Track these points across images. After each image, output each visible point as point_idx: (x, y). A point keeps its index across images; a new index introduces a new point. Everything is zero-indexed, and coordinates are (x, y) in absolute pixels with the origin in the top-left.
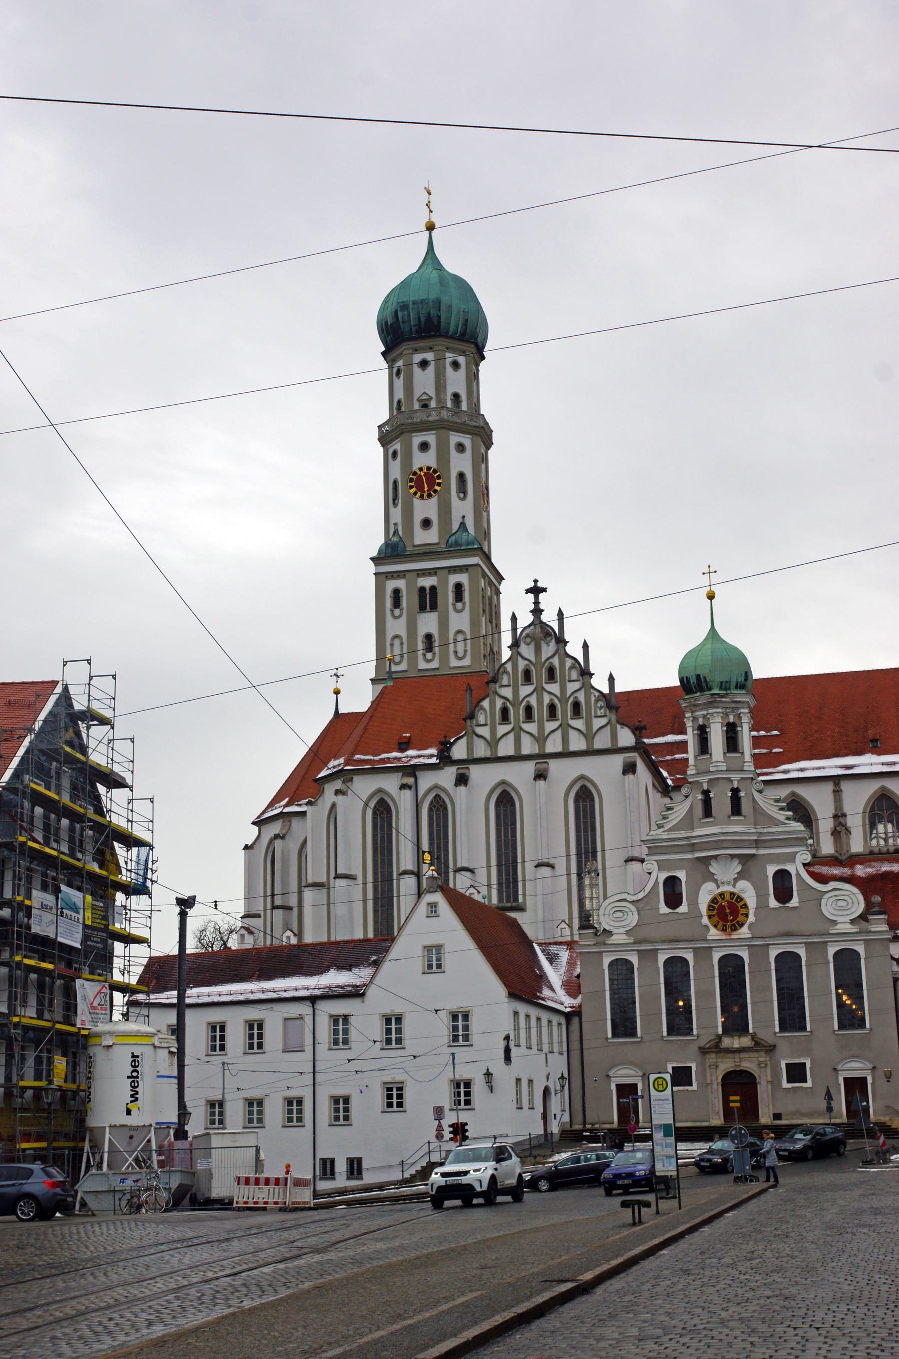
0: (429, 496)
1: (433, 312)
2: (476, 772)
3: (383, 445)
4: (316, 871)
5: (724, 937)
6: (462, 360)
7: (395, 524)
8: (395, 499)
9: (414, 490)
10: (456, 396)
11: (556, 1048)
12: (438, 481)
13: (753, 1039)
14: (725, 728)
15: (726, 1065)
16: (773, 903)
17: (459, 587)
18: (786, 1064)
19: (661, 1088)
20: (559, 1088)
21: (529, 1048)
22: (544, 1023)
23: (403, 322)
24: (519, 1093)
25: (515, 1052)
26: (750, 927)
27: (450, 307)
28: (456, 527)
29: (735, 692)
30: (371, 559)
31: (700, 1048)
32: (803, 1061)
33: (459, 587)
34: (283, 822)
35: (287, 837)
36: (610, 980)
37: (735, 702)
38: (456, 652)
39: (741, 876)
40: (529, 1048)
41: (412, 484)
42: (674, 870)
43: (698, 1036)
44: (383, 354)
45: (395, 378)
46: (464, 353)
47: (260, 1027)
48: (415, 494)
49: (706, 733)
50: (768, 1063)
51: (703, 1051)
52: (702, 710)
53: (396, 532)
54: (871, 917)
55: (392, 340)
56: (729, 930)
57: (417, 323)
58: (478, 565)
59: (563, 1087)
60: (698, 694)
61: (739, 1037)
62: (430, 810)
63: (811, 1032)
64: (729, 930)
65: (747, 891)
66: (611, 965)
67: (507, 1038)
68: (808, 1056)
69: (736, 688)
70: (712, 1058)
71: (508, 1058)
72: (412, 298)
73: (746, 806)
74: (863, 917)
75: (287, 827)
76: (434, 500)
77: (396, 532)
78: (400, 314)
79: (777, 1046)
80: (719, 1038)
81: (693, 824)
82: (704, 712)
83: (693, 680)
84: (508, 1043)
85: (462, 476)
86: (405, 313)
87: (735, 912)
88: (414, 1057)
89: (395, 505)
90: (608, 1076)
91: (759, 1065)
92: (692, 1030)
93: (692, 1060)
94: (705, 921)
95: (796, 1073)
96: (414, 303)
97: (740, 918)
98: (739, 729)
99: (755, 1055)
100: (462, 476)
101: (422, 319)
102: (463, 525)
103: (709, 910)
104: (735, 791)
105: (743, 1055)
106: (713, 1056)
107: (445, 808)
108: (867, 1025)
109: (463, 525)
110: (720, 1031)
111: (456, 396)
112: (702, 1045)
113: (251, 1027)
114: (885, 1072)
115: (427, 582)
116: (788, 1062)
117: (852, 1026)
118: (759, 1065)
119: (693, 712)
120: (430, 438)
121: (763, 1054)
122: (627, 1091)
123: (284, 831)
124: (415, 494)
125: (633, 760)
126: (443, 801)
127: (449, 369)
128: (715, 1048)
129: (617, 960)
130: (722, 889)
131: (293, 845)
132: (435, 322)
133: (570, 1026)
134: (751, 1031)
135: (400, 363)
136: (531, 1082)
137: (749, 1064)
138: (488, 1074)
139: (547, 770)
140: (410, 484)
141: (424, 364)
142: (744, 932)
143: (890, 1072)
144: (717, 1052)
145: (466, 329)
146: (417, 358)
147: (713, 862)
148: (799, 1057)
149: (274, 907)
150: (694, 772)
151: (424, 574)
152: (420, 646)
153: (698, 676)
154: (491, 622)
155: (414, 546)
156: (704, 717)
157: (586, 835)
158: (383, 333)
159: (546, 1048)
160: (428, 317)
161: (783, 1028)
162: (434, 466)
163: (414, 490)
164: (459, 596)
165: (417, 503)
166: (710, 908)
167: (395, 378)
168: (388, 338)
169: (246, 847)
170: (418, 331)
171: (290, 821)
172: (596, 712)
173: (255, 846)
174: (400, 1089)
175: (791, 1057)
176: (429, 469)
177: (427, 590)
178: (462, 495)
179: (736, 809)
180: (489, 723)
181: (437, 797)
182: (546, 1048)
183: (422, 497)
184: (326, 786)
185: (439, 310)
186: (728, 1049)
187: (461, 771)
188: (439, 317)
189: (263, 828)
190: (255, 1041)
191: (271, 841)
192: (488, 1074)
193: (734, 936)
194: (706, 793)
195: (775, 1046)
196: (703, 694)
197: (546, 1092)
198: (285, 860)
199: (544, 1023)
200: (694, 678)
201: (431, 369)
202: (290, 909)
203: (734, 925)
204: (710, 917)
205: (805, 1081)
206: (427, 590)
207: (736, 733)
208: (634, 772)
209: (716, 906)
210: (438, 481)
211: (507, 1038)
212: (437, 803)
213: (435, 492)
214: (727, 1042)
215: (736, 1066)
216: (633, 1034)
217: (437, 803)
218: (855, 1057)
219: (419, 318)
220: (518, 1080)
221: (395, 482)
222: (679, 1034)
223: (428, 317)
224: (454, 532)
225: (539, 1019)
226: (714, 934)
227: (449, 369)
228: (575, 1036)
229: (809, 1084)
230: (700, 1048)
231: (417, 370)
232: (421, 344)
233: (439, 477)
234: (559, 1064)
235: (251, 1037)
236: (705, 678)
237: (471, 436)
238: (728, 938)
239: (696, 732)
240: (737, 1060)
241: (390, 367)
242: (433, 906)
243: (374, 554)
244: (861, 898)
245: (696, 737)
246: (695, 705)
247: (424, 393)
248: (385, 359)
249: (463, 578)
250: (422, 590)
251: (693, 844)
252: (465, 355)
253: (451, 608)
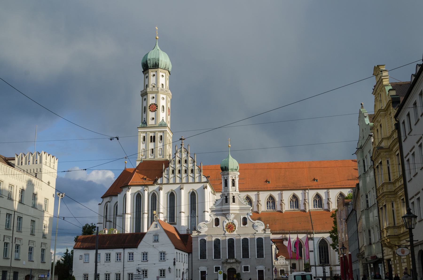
1: (157, 62)
2: (164, 187)
3: (142, 97)
4: (120, 212)
5: (229, 234)
6: (164, 75)
7: (144, 118)
8: (144, 112)
11: (186, 262)
13: (235, 260)
14: (232, 180)
15: (228, 267)
16: (242, 225)
18: (244, 267)
19: (220, 273)
20: (186, 272)
21: (180, 262)
22: (183, 255)
23: (149, 64)
24: (177, 273)
25: (176, 263)
26: (236, 232)
27: (162, 61)
28: (161, 120)
29: (234, 171)
31: (222, 262)
32: (248, 266)
33: (161, 136)
34: (110, 198)
35: (111, 202)
36: (200, 244)
37: (235, 174)
38: (159, 154)
39: (235, 218)
40: (180, 262)
42: (218, 216)
43: (222, 259)
44: (143, 72)
45: (146, 79)
47: (110, 255)
49: (227, 181)
50: (239, 266)
51: (223, 263)
52: (226, 175)
53: (145, 120)
54: (266, 230)
55: (145, 68)
56: (231, 232)
57: (153, 64)
58: (167, 131)
59: (187, 271)
60: (225, 171)
61: (232, 259)
62: (152, 197)
63: (250, 258)
64: (231, 232)
65: (236, 222)
66: (200, 240)
67: (174, 259)
68: (249, 264)
69: (235, 170)
70: (225, 265)
71: (174, 264)
72: (151, 58)
73: (236, 200)
74: (264, 230)
75: (111, 199)
77: (145, 120)
78: (148, 62)
79: (242, 262)
80: (227, 259)
81: (222, 205)
82: (227, 176)
83: (224, 168)
84: (175, 260)
86: (150, 61)
87: (233, 228)
88: (155, 264)
89: (145, 113)
90: (198, 269)
91: (237, 267)
92: (220, 257)
93: (220, 265)
94: (225, 230)
95: (246, 269)
96: (152, 59)
97: (234, 229)
98: (235, 181)
99: (236, 264)
100: (163, 106)
101: (154, 63)
102: (163, 119)
103: (226, 227)
104: (234, 197)
105: (233, 264)
106: (226, 264)
107: (156, 197)
108: (264, 257)
109: (163, 119)
110: (227, 258)
111: (163, 85)
112: (223, 261)
113: (107, 255)
114: (268, 269)
115: (152, 135)
116: (244, 266)
117: (260, 257)
118: (237, 267)
119: (224, 176)
120: (154, 95)
121: (238, 264)
122: (203, 273)
123: (110, 200)
125: (206, 185)
126: (155, 194)
127: (161, 77)
128: (226, 262)
129: (202, 239)
130: (229, 222)
131: (112, 204)
132: (157, 64)
133: (189, 256)
134: (235, 258)
135: (147, 75)
136: (180, 270)
137: (234, 266)
138: (169, 268)
139: (183, 187)
142: (235, 233)
143: (269, 269)
144: (226, 263)
145: (166, 67)
147: (227, 214)
148: (247, 265)
149: (106, 221)
150: (224, 191)
151: (152, 132)
152: (150, 152)
153: (225, 167)
154: (169, 146)
156: (227, 177)
157: (193, 205)
158: (143, 66)
159: (183, 262)
160: (156, 63)
161: (243, 258)
164: (161, 139)
165: (150, 112)
166: (226, 226)
167: (146, 79)
168: (145, 68)
169: (99, 204)
170: (153, 67)
171: (112, 197)
172: (196, 172)
173: (102, 204)
174: (146, 271)
175: (245, 265)
176: (154, 104)
177: (153, 137)
178: (163, 111)
179: (234, 201)
180: (168, 174)
181: (154, 193)
182: (183, 262)
183: (152, 111)
184: (123, 189)
185: (159, 61)
186: (229, 262)
187: (160, 187)
188: (159, 63)
189: (104, 199)
190: (108, 259)
191: (106, 203)
192: (169, 268)
193: (232, 233)
194: (226, 197)
195: (241, 262)
196: (227, 171)
197: (183, 273)
198: (110, 208)
199: (183, 255)
200: (224, 167)
202: (111, 222)
203: (232, 231)
204: (226, 229)
205: (248, 271)
206: (153, 137)
207: (234, 182)
208: (207, 189)
209: (228, 226)
211: (174, 259)
212: (154, 195)
214: (229, 261)
215: (231, 267)
216: (206, 258)
217: (154, 195)
218: (261, 265)
219: (153, 63)
220: (177, 270)
222: (217, 258)
223: (156, 63)
225: (182, 254)
226: (227, 233)
228: (190, 259)
229: (249, 272)
230: (222, 262)
234: (186, 266)
235: (107, 257)
236: (227, 167)
237: (166, 96)
238: (230, 234)
239: (224, 181)
240: (232, 265)
241: (145, 75)
242: (156, 225)
244: (264, 225)
245: (224, 182)
246: (224, 174)
248: (143, 73)
251: (222, 210)
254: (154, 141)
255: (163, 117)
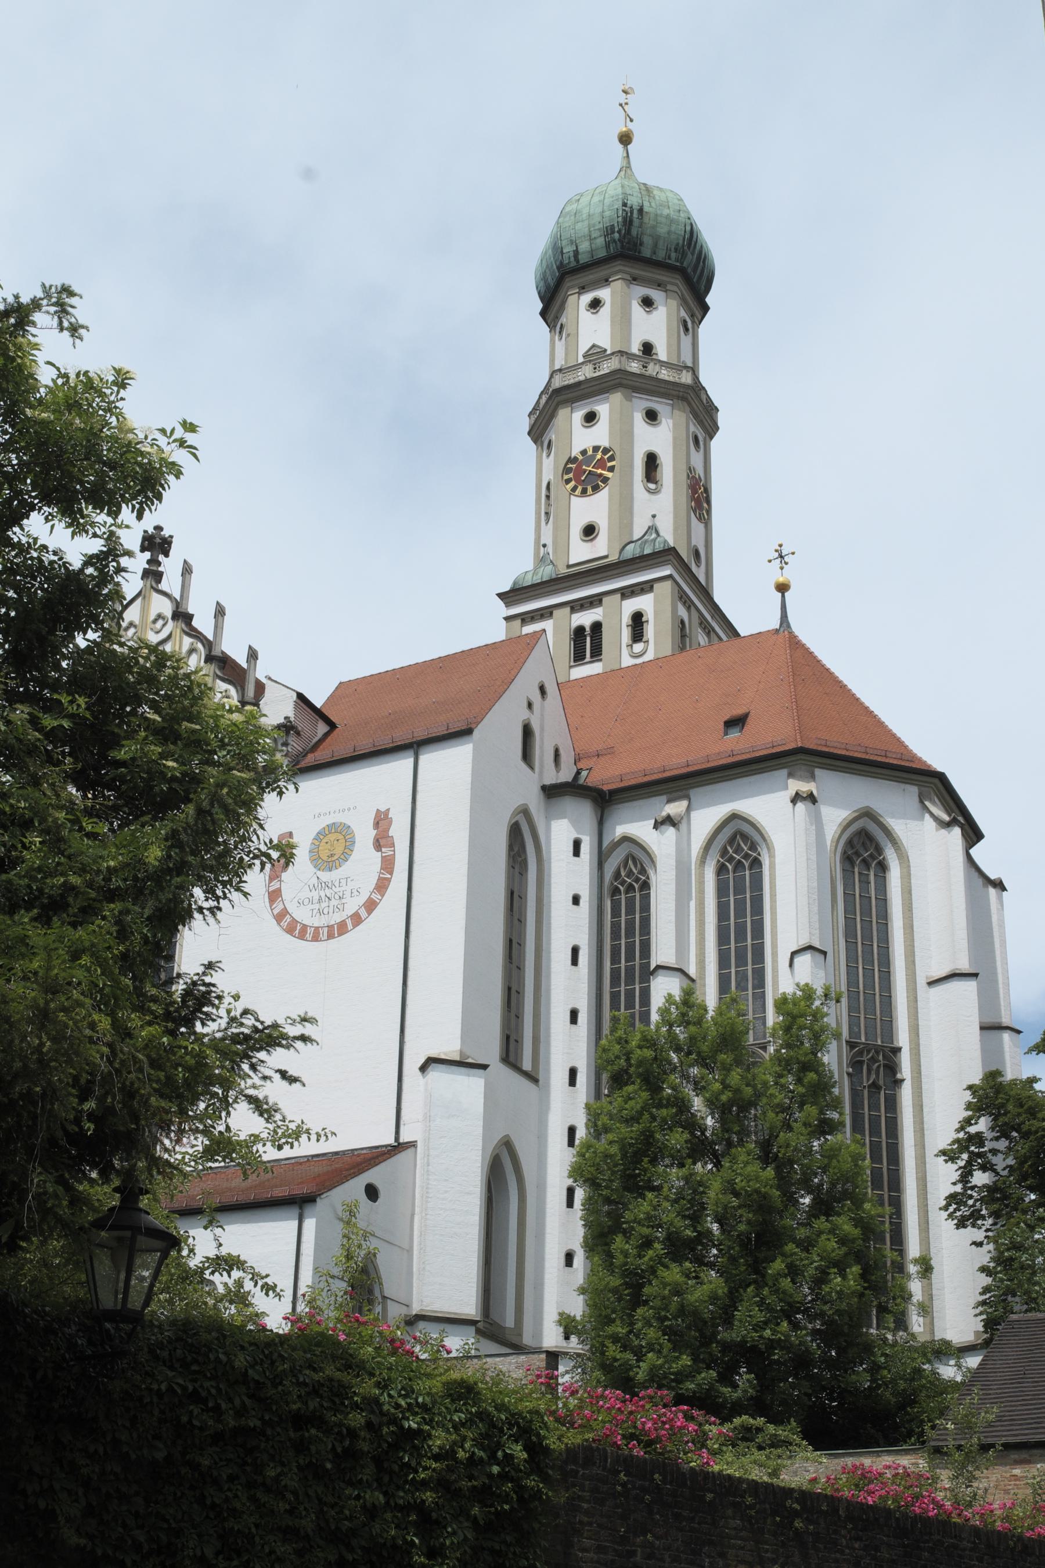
0: (596, 489)
3: (535, 442)
9: (573, 483)
10: (648, 348)
12: (609, 464)
17: (638, 619)
30: (500, 595)
33: (638, 619)
41: (571, 475)
44: (544, 314)
46: (659, 285)
48: (574, 489)
76: (604, 494)
85: (652, 461)
102: (653, 529)
109: (653, 529)
115: (585, 619)
124: (574, 489)
140: (566, 477)
141: (595, 304)
146: (587, 298)
155: (569, 566)
162: (605, 443)
163: (573, 483)
176: (596, 449)
177: (588, 629)
178: (652, 486)
183: (584, 492)
201: (605, 310)
206: (588, 629)
210: (609, 464)
213: (605, 480)
221: (549, 484)
224: (635, 538)
227: (637, 310)
231: (585, 316)
232: (591, 277)
233: (612, 458)
243: (507, 589)
247: (594, 346)
249: (644, 603)
250: (580, 631)
252: (666, 291)
253: (625, 651)
254: (597, 652)
255: (654, 516)
